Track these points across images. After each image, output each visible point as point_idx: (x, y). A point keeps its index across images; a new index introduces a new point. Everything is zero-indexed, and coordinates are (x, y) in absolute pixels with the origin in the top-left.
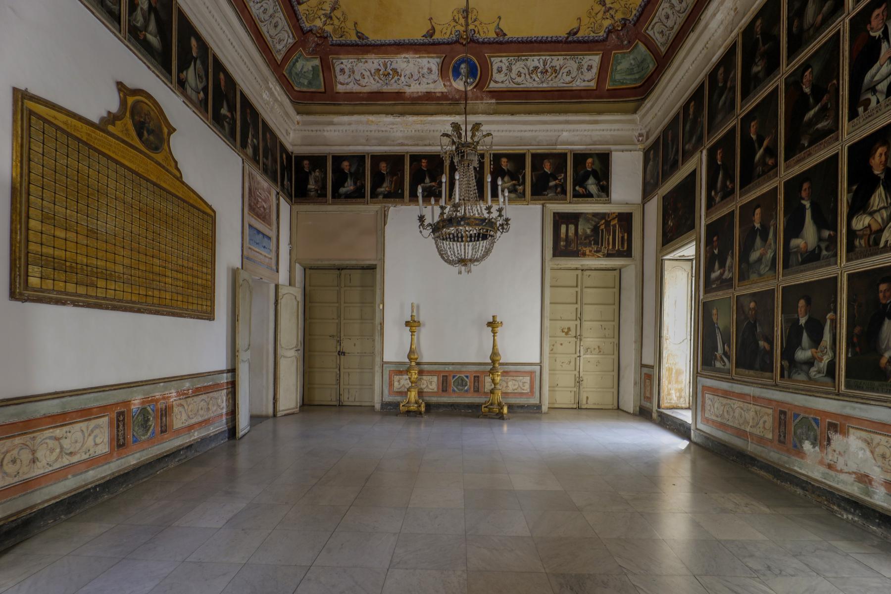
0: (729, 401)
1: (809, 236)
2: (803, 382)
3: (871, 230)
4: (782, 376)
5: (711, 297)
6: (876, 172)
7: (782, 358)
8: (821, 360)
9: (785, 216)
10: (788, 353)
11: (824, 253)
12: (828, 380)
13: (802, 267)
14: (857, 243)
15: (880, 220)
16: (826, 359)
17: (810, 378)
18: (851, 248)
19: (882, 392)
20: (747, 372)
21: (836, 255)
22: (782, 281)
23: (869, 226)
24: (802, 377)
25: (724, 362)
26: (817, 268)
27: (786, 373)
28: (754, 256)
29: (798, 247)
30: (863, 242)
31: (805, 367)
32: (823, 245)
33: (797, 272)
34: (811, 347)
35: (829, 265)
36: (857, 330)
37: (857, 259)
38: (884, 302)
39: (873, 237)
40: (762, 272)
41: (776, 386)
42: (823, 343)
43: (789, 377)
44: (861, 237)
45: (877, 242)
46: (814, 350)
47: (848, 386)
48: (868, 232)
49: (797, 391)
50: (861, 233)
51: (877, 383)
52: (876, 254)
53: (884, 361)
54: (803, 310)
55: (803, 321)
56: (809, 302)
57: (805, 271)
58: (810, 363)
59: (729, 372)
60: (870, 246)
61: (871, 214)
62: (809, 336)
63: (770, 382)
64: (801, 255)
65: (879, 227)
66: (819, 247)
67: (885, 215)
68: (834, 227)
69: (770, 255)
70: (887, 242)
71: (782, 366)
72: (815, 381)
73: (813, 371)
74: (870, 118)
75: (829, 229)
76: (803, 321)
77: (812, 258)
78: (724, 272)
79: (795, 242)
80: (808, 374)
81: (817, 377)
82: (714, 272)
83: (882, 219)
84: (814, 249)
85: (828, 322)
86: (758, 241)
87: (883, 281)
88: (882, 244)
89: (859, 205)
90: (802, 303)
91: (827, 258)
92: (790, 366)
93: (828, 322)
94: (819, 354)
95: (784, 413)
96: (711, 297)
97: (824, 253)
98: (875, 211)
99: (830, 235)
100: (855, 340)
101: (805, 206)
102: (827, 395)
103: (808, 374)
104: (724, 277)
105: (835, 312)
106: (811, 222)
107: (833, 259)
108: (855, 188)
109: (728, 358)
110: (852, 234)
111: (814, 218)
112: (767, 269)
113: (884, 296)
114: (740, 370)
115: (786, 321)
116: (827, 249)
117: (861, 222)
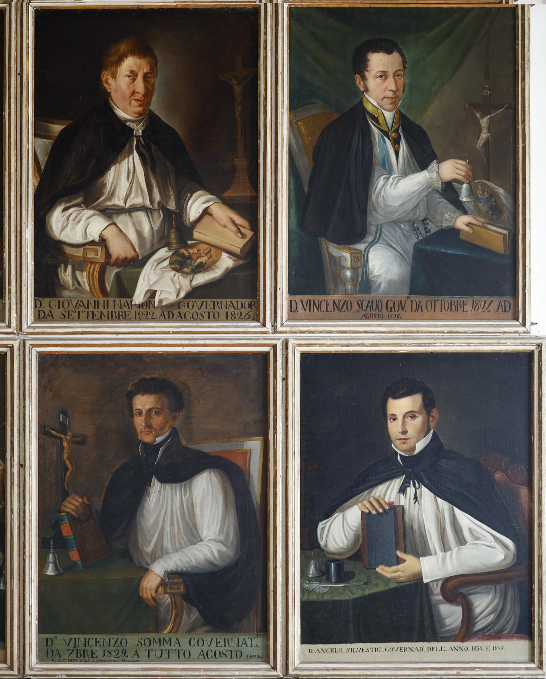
3: (108, 255)
6: (121, 113)
14: (66, 275)
15: (133, 236)
18: (47, 285)
23: (103, 241)
37: (67, 317)
39: (112, 273)
45: (125, 289)
48: (100, 257)
50: (79, 253)
61: (109, 213)
65: (130, 254)
67: (146, 229)
70: (152, 294)
83: (139, 234)
88: (139, 297)
89: (71, 176)
98: (120, 211)
108: (57, 128)
110: (49, 251)
117: (74, 226)
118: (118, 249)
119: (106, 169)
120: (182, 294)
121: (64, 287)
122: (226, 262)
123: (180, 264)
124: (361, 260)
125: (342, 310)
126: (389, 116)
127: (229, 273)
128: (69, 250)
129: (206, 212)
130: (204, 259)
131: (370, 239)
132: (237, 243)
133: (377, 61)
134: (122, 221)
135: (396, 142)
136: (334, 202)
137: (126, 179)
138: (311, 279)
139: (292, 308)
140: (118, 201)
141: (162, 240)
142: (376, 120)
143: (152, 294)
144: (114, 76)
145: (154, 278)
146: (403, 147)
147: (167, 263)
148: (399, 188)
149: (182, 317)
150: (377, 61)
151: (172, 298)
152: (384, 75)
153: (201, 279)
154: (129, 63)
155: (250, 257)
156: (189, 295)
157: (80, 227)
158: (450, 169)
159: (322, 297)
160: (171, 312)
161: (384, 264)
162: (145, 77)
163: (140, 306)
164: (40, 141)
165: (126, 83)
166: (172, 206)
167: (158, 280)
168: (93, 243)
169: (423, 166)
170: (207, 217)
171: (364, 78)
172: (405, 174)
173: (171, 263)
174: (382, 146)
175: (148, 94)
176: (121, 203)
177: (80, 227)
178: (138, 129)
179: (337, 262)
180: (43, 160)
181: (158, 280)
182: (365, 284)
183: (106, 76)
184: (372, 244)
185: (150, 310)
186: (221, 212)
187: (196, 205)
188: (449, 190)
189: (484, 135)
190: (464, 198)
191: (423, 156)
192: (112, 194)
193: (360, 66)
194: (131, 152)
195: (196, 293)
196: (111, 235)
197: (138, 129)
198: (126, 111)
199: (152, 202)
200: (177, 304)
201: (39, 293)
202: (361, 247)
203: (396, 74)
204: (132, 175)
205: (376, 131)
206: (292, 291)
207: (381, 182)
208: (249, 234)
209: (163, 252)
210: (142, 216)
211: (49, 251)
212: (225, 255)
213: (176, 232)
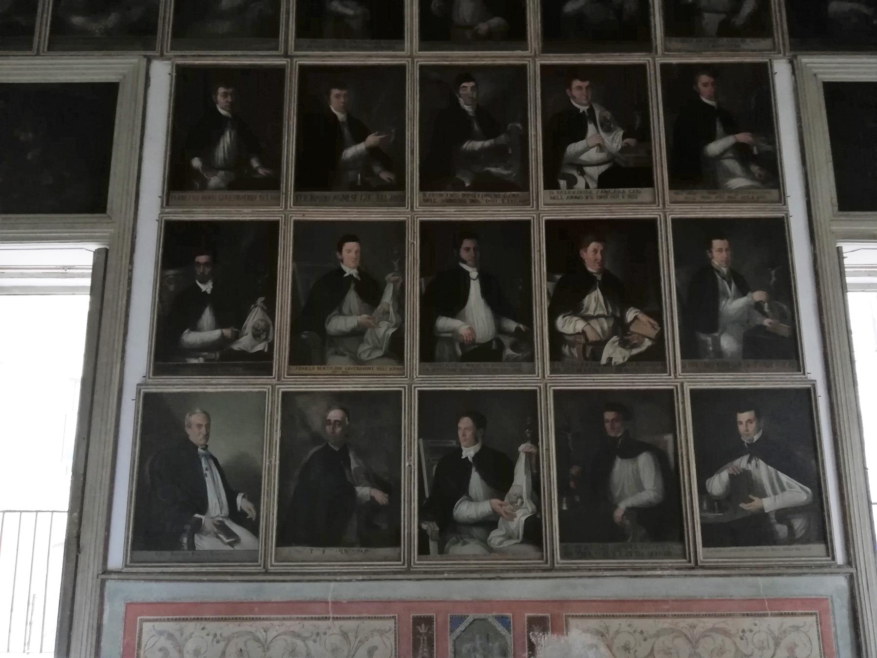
0: (246, 626)
1: (476, 318)
2: (475, 557)
3: (587, 339)
4: (424, 550)
5: (174, 385)
6: (590, 269)
7: (422, 517)
8: (512, 517)
9: (423, 273)
10: (438, 506)
11: (509, 352)
12: (529, 549)
13: (464, 365)
14: (566, 350)
15: (599, 330)
16: (521, 516)
17: (491, 550)
18: (556, 355)
19: (621, 557)
20: (317, 552)
21: (531, 359)
22: (412, 381)
23: (583, 333)
24: (472, 548)
25: (229, 533)
26: (495, 372)
27: (433, 546)
28: (338, 324)
29: (454, 331)
30: (575, 351)
31: (477, 532)
32: (507, 341)
33: (453, 371)
34: (489, 497)
35: (519, 371)
36: (574, 470)
37: (567, 371)
38: (612, 434)
39: (589, 349)
40: (364, 357)
41: (408, 572)
42: (513, 490)
43: (442, 551)
44: (572, 345)
45: (596, 355)
46: (496, 501)
47: (565, 555)
48: (583, 340)
49: (460, 574)
50: (571, 338)
51: (611, 545)
52: (597, 372)
53: (619, 513)
54: (469, 434)
55: (469, 452)
56: (480, 422)
57: (471, 372)
58: (489, 523)
59: (251, 557)
60: (586, 358)
61: (587, 319)
62: (484, 477)
63: (396, 565)
64: (462, 345)
65: (598, 339)
66: (498, 341)
67: (606, 326)
68: (526, 317)
69: (385, 330)
70: (610, 359)
71: (422, 534)
72: (502, 553)
73: (496, 537)
74: (576, 201)
75: (515, 319)
76: (469, 452)
77: (482, 354)
78: (237, 337)
79: (444, 323)
80: (484, 542)
81: (506, 544)
82: (195, 328)
83: (602, 328)
84: (490, 342)
85: (522, 458)
86: (352, 298)
87: (611, 407)
88: (604, 361)
89: (566, 300)
90: (465, 423)
91: (515, 360)
92: (442, 531)
93: (522, 458)
94: (508, 508)
95: (428, 621)
96: (174, 385)
97: (509, 352)
98: (593, 317)
99: (518, 329)
100: (572, 484)
101: (468, 273)
102: (526, 572)
103: (484, 542)
104: (236, 347)
105: (535, 441)
106: (482, 302)
107: (525, 365)
108: (558, 277)
109: (253, 527)
110: (557, 339)
111: (486, 293)
112: (379, 353)
113: (613, 428)
114: (286, 550)
115: (430, 450)
116: (514, 347)
117: (569, 325)
118: (592, 337)
119: (584, 297)
120: (626, 359)
121: (564, 355)
122: (648, 343)
123: (624, 344)
124: (717, 342)
125: (708, 368)
126: (724, 270)
127: (649, 349)
128: (567, 338)
129: (636, 318)
130: (636, 341)
131: (720, 331)
132: (653, 333)
133: (717, 244)
134: (594, 323)
135: (729, 284)
136: (700, 312)
137: (594, 301)
138: (692, 351)
139: (683, 367)
140: (591, 312)
141: (613, 331)
142: (718, 272)
143: (610, 359)
144: (586, 251)
145: (611, 351)
146: (733, 285)
147: (617, 343)
148: (733, 305)
149: (627, 372)
150: (717, 244)
151: (621, 361)
152: (720, 250)
153: (635, 351)
154: (593, 245)
155: (660, 340)
156: (629, 360)
157: (572, 326)
158: (758, 296)
159: (698, 360)
160: (620, 369)
161: (728, 343)
162: (601, 251)
163: (604, 365)
164: (550, 283)
165: (592, 255)
166: (618, 315)
167: (613, 352)
168: (578, 333)
169: (744, 295)
170: (636, 321)
171: (711, 252)
172: (736, 297)
173: (619, 344)
174: (723, 284)
175: (603, 261)
176: (592, 314)
177: (572, 326)
178: (599, 277)
179: (705, 343)
180: (551, 291)
181: (613, 352)
182: (719, 352)
183: (582, 252)
184: (722, 333)
185: (610, 367)
186: (644, 318)
187: (630, 315)
188: (758, 306)
189: (774, 279)
190: (766, 310)
191: (743, 290)
192: (587, 309)
193: (709, 246)
194: (596, 289)
195: (632, 359)
196: (588, 330)
197: (599, 277)
198: (592, 268)
199: (608, 312)
200: (623, 365)
201: (552, 359)
202: (716, 334)
203: (726, 250)
204: (597, 300)
205: (719, 277)
206: (683, 357)
207: (724, 302)
208: (659, 329)
209: (615, 338)
210: (603, 320)
211: (557, 339)
212: (647, 340)
213: (621, 328)
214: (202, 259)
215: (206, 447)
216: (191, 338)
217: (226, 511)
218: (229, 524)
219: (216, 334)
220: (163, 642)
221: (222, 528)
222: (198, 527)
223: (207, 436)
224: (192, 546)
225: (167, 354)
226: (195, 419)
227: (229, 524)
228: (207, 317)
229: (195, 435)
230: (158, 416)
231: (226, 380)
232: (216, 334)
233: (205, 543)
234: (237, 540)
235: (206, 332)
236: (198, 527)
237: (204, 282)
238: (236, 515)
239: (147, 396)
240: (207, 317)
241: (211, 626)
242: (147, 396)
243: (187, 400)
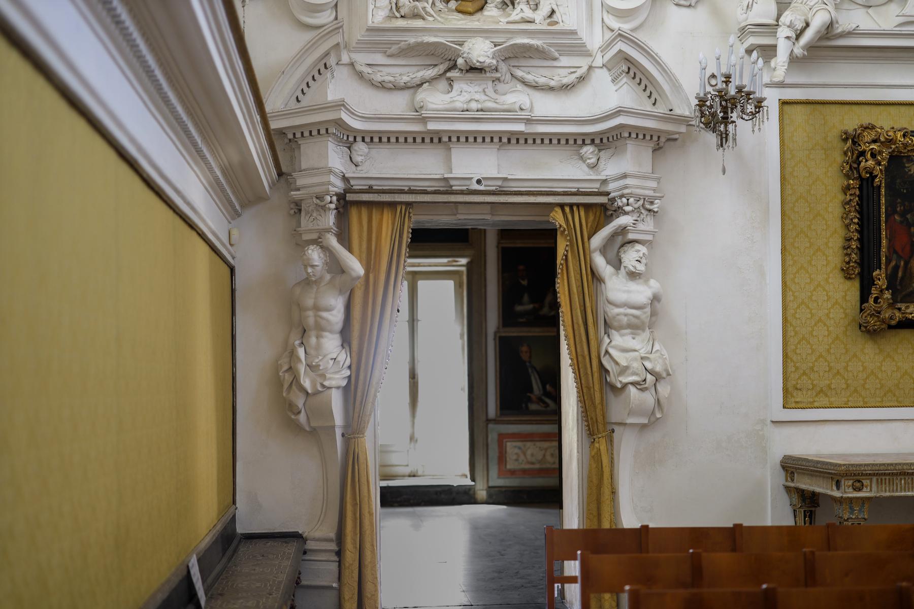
5: (513, 332)
25: (544, 403)
82: (521, 304)
96: (513, 332)
104: (542, 313)
214: (521, 267)
215: (530, 362)
216: (519, 308)
217: (542, 392)
218: (543, 398)
219: (531, 306)
220: (517, 451)
221: (540, 400)
222: (530, 400)
223: (530, 357)
224: (527, 407)
225: (508, 317)
226: (524, 348)
227: (543, 398)
228: (526, 298)
229: (525, 357)
230: (506, 347)
231: (537, 329)
232: (531, 306)
233: (533, 407)
234: (547, 405)
235: (525, 306)
236: (530, 400)
237: (523, 280)
238: (547, 394)
239: (501, 338)
240: (526, 298)
241: (538, 444)
242: (501, 338)
243: (520, 340)
